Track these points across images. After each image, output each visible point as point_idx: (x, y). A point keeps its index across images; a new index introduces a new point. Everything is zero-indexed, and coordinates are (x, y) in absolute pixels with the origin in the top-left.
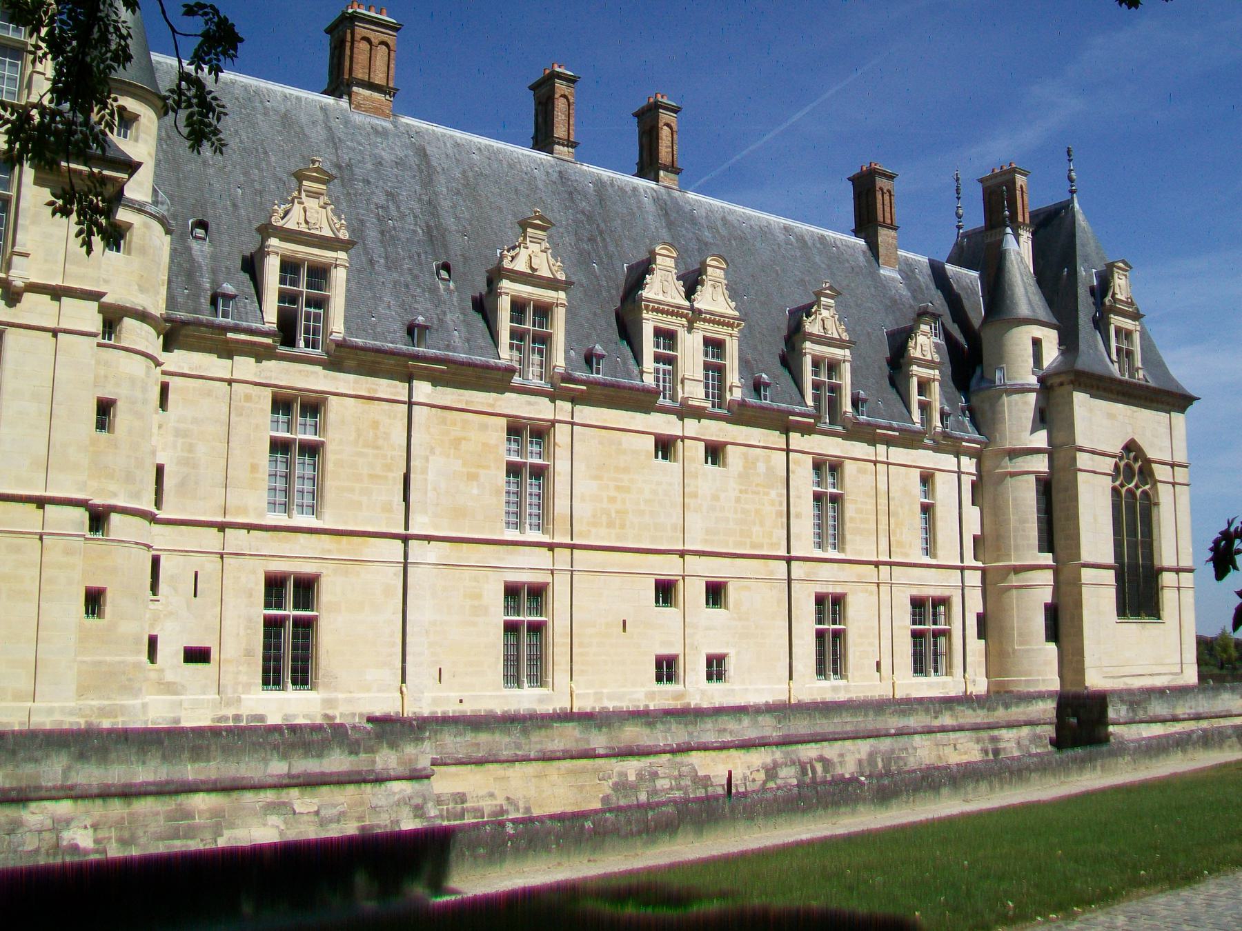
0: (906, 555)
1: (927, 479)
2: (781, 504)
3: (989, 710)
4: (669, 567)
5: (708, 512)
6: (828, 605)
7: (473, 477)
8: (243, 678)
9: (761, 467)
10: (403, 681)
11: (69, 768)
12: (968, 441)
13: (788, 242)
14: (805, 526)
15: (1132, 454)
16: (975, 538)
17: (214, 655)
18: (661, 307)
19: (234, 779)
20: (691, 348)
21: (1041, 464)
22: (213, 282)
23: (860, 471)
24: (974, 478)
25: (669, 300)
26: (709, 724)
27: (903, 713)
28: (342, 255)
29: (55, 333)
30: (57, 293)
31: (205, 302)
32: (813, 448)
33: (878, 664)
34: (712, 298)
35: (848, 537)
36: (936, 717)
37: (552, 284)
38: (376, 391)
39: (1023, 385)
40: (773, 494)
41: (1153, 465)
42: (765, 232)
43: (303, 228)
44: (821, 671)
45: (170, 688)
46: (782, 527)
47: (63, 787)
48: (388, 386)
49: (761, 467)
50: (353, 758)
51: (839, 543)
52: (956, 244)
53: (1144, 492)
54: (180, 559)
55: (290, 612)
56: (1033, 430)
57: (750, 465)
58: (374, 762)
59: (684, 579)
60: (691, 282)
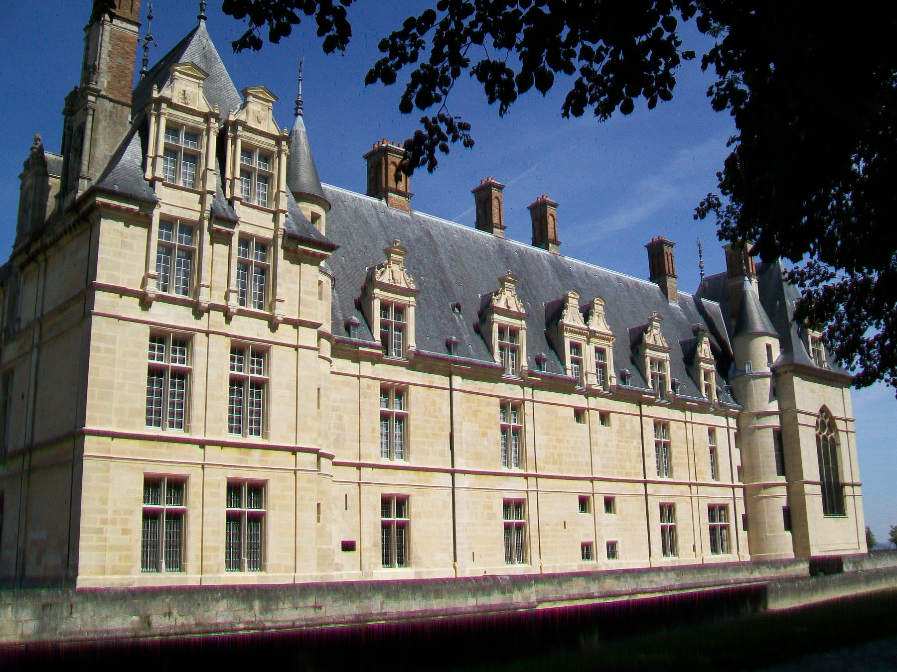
1: (712, 432)
4: (585, 488)
7: (484, 434)
8: (373, 560)
10: (455, 560)
11: (383, 602)
12: (733, 408)
13: (620, 287)
14: (652, 462)
15: (824, 414)
16: (738, 467)
17: (357, 546)
19: (455, 609)
20: (588, 352)
21: (775, 421)
22: (344, 316)
23: (678, 427)
24: (736, 431)
25: (576, 324)
26: (645, 578)
28: (412, 299)
29: (297, 348)
30: (296, 324)
31: (342, 328)
33: (694, 547)
34: (598, 324)
35: (674, 468)
36: (752, 573)
37: (518, 316)
39: (763, 373)
41: (837, 421)
42: (607, 280)
43: (392, 282)
44: (665, 552)
47: (381, 614)
48: (439, 379)
49: (628, 426)
50: (502, 596)
51: (669, 471)
52: (701, 285)
53: (832, 437)
55: (394, 518)
56: (770, 401)
57: (622, 424)
58: (512, 598)
59: (593, 496)
60: (587, 312)
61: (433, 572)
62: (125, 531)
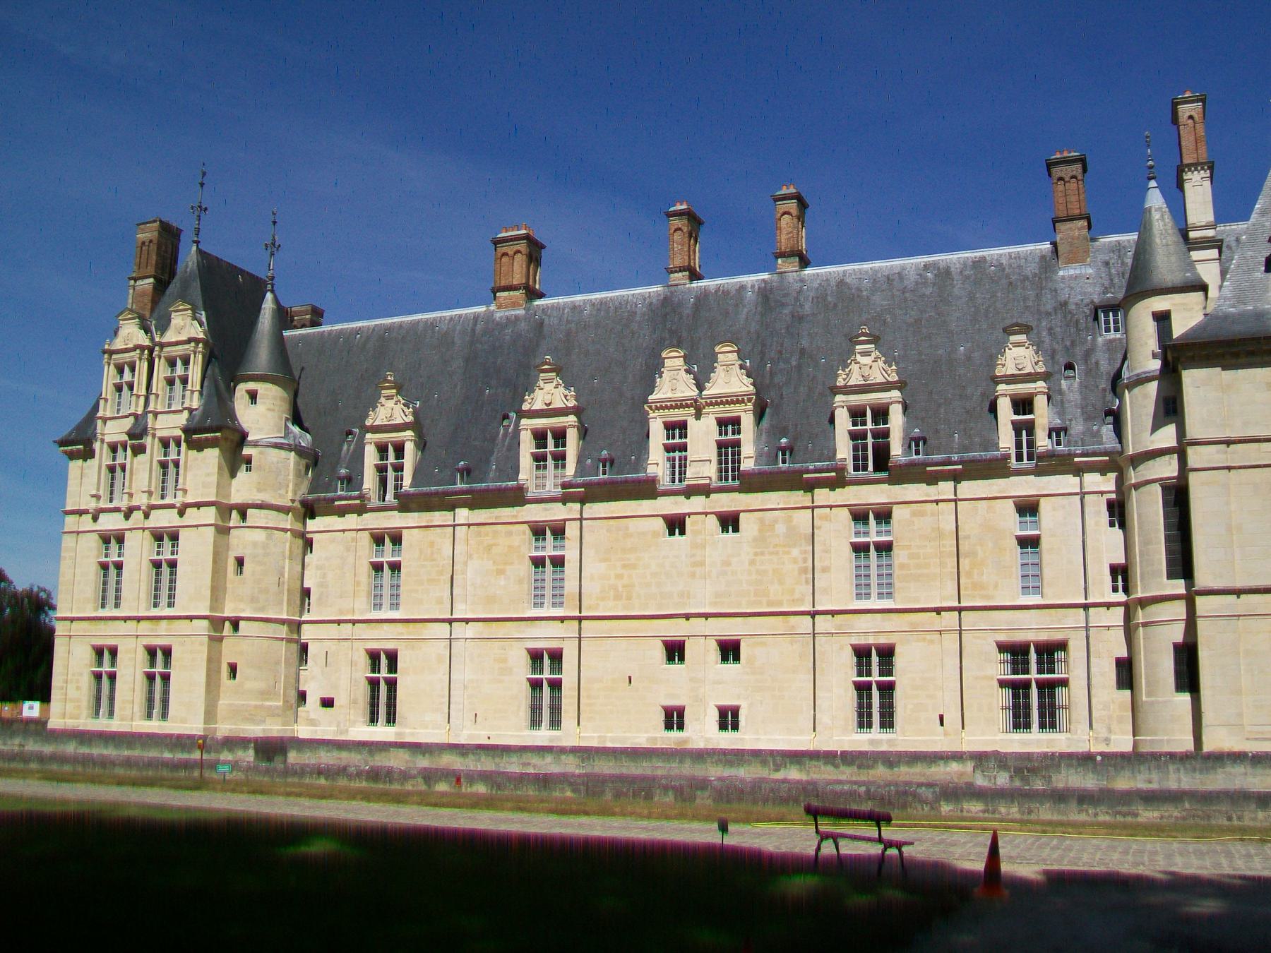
2: (805, 560)
3: (859, 767)
4: (675, 630)
5: (718, 577)
7: (500, 572)
9: (781, 528)
12: (1082, 455)
18: (669, 404)
26: (514, 758)
27: (730, 763)
32: (848, 500)
35: (897, 584)
38: (432, 521)
39: (1138, 375)
40: (795, 552)
45: (312, 722)
46: (807, 582)
49: (781, 528)
54: (318, 644)
56: (1155, 428)
61: (418, 733)
62: (78, 688)
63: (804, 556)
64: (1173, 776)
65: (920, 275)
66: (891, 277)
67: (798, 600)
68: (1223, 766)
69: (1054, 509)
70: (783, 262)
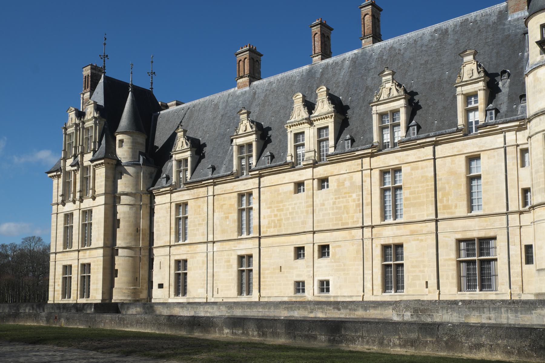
0: (451, 213)
2: (359, 200)
4: (299, 241)
5: (319, 212)
6: (392, 251)
9: (347, 184)
40: (354, 196)
46: (360, 212)
49: (347, 184)
63: (358, 197)
64: (504, 315)
65: (432, 36)
66: (417, 40)
67: (356, 221)
68: (535, 308)
69: (489, 158)
70: (365, 42)
